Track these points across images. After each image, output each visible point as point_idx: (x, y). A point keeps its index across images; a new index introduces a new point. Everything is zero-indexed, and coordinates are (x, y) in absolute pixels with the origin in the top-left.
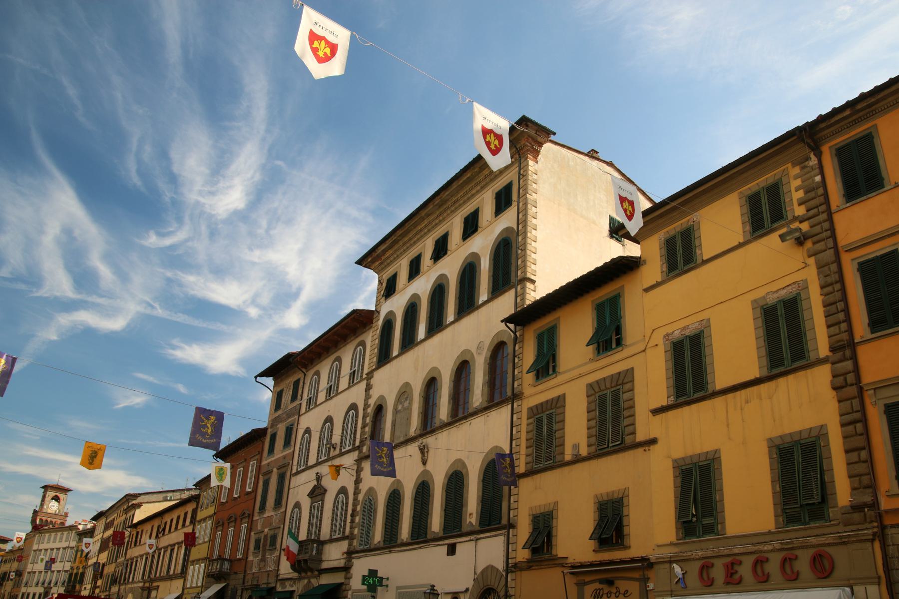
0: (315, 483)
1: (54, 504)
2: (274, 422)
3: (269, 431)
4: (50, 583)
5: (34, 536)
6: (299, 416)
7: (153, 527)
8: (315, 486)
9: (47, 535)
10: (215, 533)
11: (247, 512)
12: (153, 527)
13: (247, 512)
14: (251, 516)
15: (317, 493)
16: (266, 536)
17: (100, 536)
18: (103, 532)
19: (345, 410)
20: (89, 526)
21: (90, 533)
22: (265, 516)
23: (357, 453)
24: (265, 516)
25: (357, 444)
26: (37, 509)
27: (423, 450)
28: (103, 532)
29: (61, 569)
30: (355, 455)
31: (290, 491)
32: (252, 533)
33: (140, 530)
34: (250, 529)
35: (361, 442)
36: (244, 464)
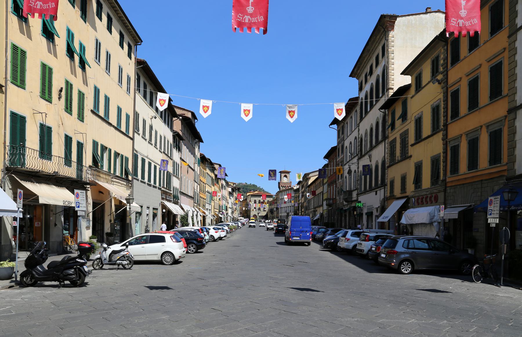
0: (349, 169)
1: (285, 178)
2: (338, 143)
3: (338, 147)
4: (288, 211)
5: (279, 193)
6: (344, 141)
7: (314, 186)
8: (349, 170)
9: (283, 192)
10: (328, 189)
11: (335, 180)
12: (314, 186)
13: (335, 180)
14: (336, 182)
15: (350, 172)
16: (340, 189)
17: (301, 191)
18: (302, 189)
19: (354, 139)
20: (298, 187)
21: (298, 190)
22: (339, 181)
23: (357, 157)
24: (339, 181)
25: (357, 153)
26: (279, 182)
27: (370, 157)
28: (302, 189)
29: (291, 205)
30: (357, 158)
31: (344, 171)
32: (337, 188)
33: (310, 188)
34: (336, 186)
35: (358, 152)
36: (333, 161)
